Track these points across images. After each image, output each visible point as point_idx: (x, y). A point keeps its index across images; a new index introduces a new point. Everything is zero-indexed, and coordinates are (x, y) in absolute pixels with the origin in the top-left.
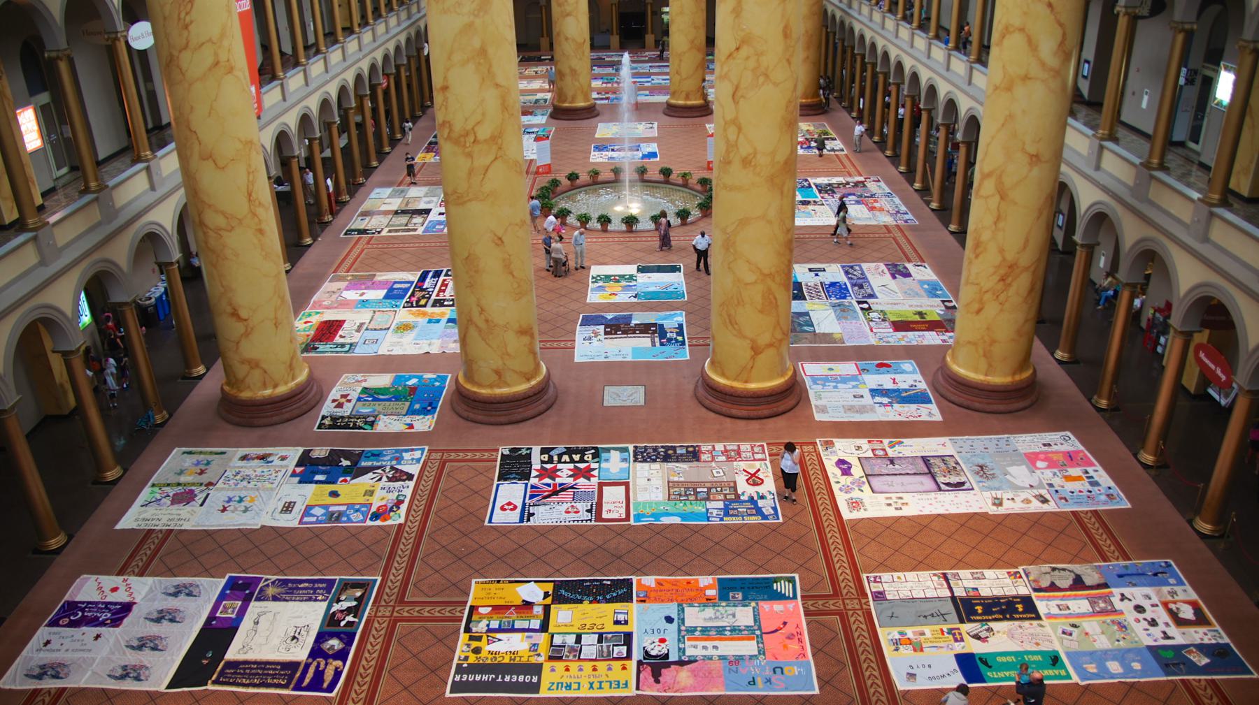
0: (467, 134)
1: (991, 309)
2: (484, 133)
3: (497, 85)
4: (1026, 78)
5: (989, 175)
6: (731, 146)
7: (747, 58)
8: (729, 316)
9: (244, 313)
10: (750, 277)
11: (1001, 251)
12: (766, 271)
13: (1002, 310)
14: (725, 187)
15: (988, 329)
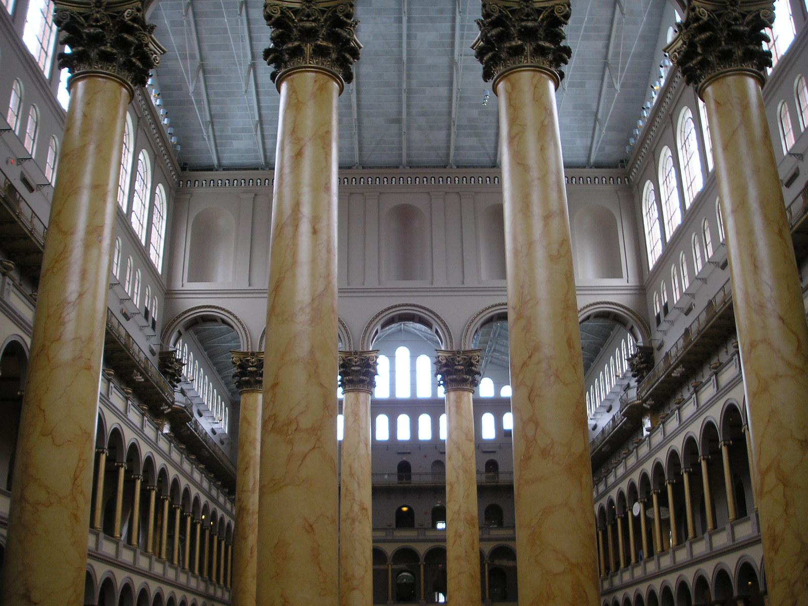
0: (291, 423)
2: (305, 422)
3: (322, 385)
4: (776, 377)
9: (36, 596)
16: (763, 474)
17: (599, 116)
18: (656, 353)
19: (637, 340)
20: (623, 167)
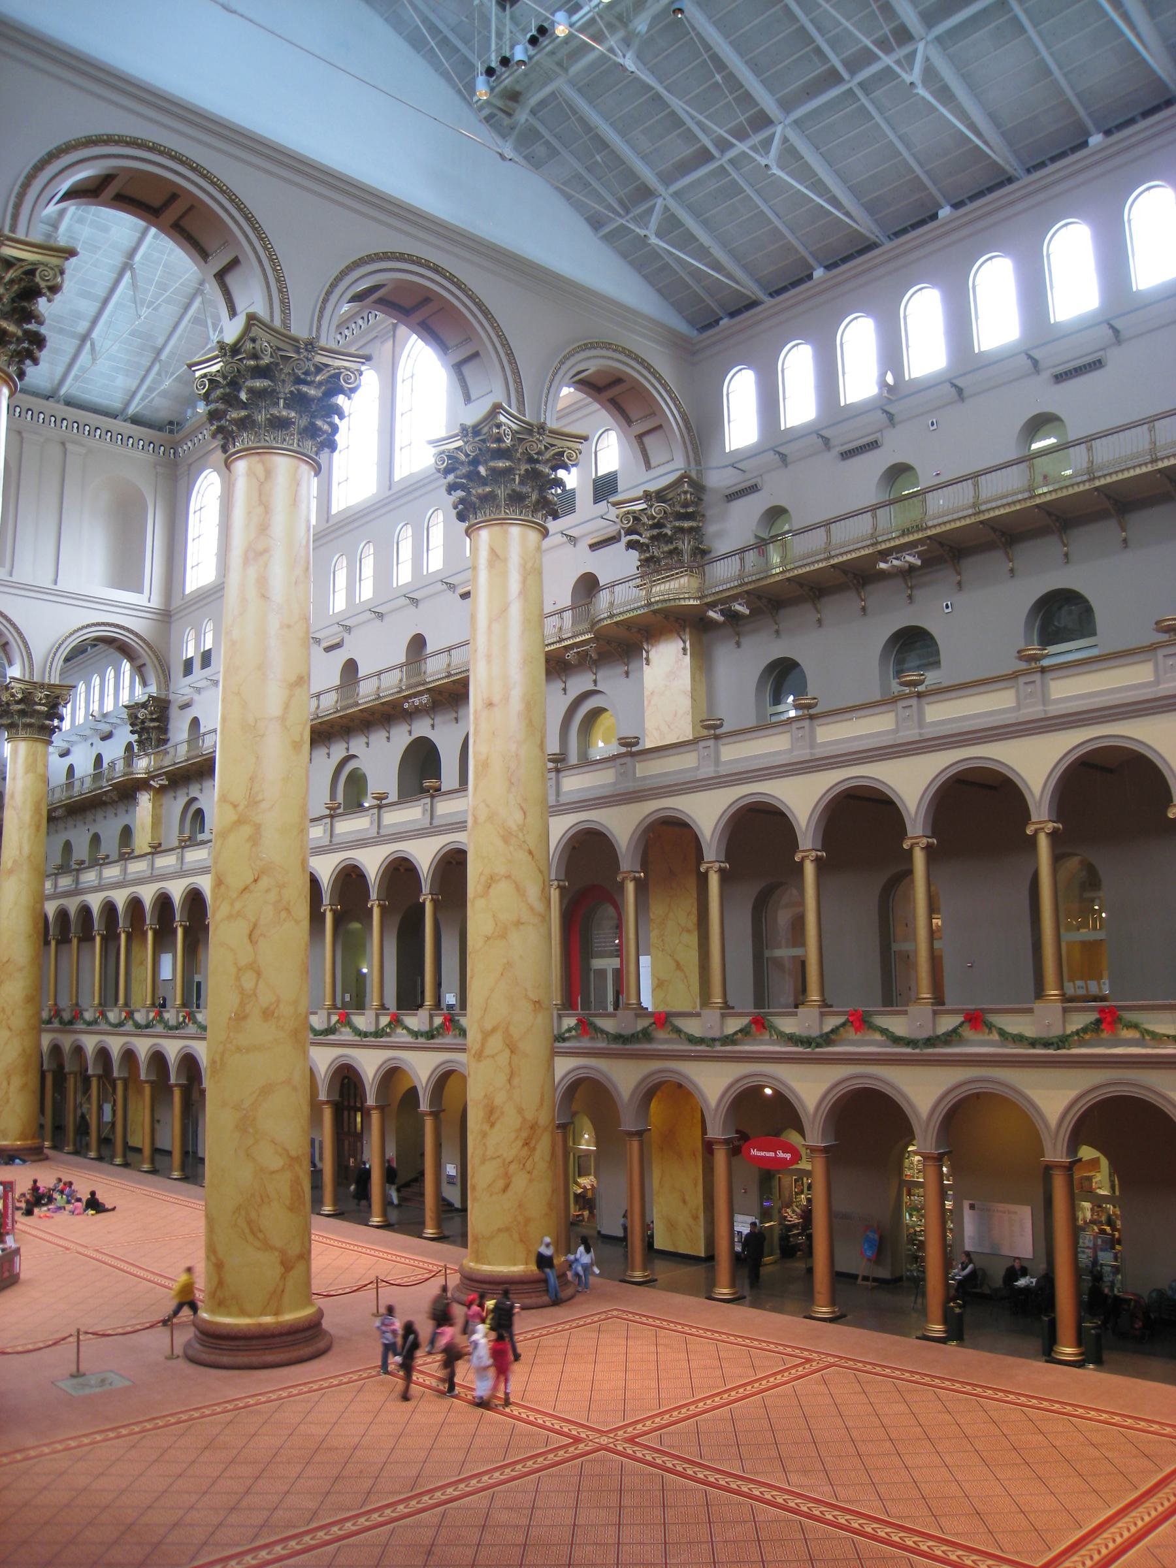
1: (520, 1182)
4: (518, 923)
5: (494, 1030)
6: (246, 997)
7: (268, 890)
8: (249, 1223)
10: (277, 1163)
11: (520, 1111)
12: (293, 1153)
13: (531, 1181)
14: (239, 1049)
15: (520, 1206)
16: (486, 1035)
17: (164, 356)
18: (174, 712)
19: (145, 684)
20: (171, 432)
